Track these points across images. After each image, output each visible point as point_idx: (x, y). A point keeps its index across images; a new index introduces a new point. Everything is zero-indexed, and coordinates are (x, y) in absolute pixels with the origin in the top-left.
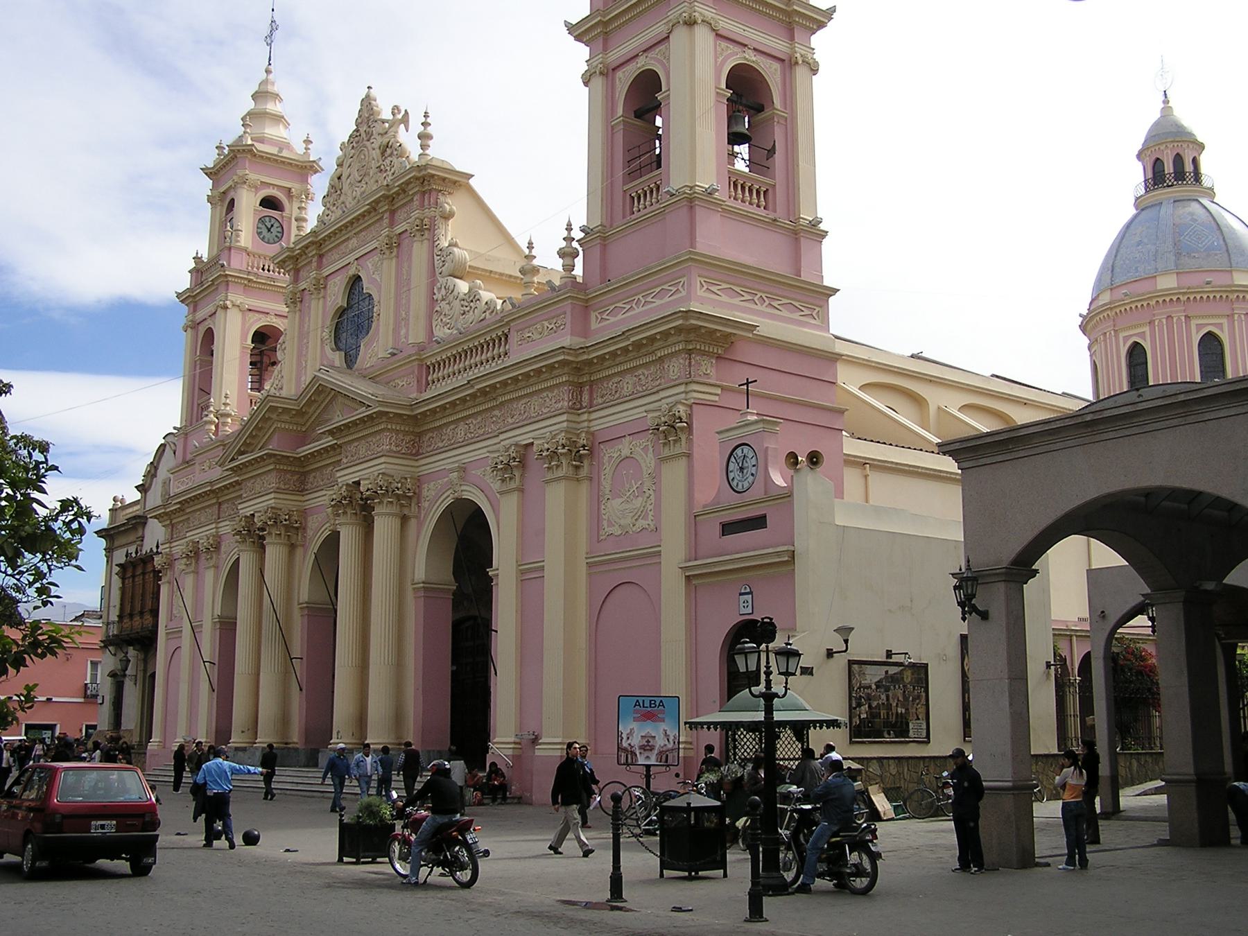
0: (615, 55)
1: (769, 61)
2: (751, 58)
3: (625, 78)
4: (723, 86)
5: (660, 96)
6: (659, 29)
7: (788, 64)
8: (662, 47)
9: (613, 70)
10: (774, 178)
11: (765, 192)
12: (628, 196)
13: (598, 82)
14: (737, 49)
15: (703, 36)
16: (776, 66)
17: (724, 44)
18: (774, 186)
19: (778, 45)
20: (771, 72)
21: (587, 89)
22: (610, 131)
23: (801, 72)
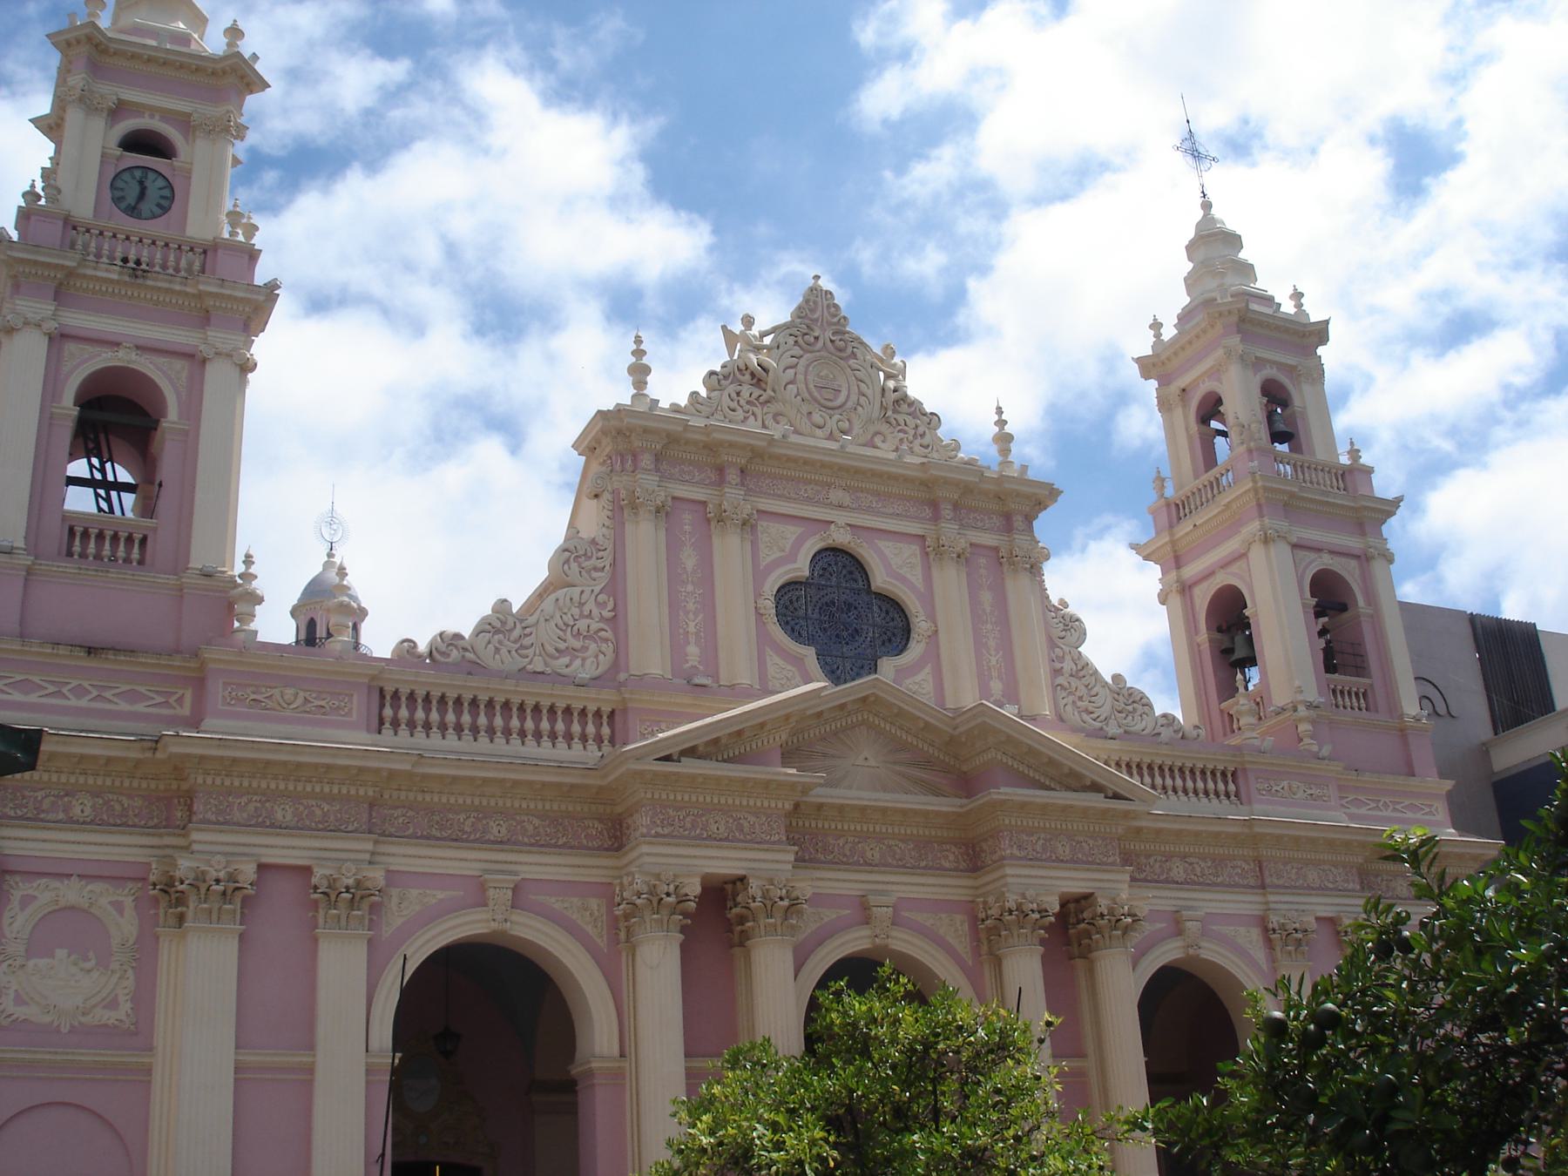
0: (1191, 571)
1: (1343, 560)
2: (1326, 561)
3: (1203, 596)
4: (1308, 594)
5: (1247, 612)
6: (1232, 546)
7: (1364, 558)
8: (1241, 564)
9: (1190, 587)
10: (1370, 677)
11: (1365, 694)
12: (1226, 715)
13: (1176, 600)
14: (1313, 555)
15: (1282, 551)
16: (1353, 563)
17: (1301, 553)
18: (1372, 685)
19: (1352, 542)
20: (1348, 570)
21: (1165, 607)
22: (1194, 649)
23: (1377, 566)
